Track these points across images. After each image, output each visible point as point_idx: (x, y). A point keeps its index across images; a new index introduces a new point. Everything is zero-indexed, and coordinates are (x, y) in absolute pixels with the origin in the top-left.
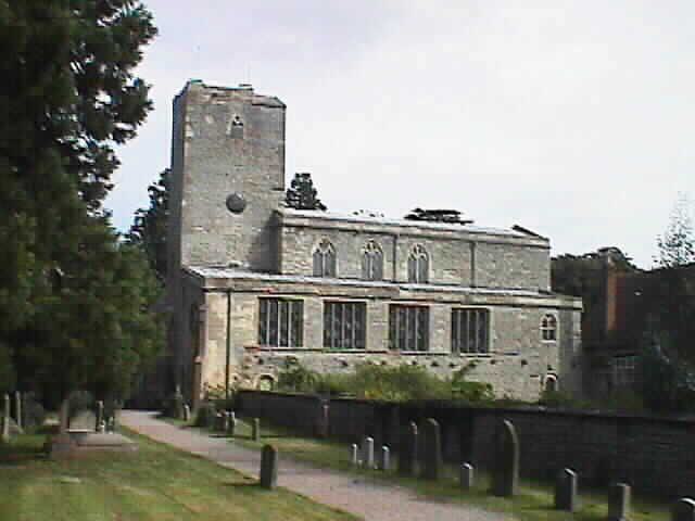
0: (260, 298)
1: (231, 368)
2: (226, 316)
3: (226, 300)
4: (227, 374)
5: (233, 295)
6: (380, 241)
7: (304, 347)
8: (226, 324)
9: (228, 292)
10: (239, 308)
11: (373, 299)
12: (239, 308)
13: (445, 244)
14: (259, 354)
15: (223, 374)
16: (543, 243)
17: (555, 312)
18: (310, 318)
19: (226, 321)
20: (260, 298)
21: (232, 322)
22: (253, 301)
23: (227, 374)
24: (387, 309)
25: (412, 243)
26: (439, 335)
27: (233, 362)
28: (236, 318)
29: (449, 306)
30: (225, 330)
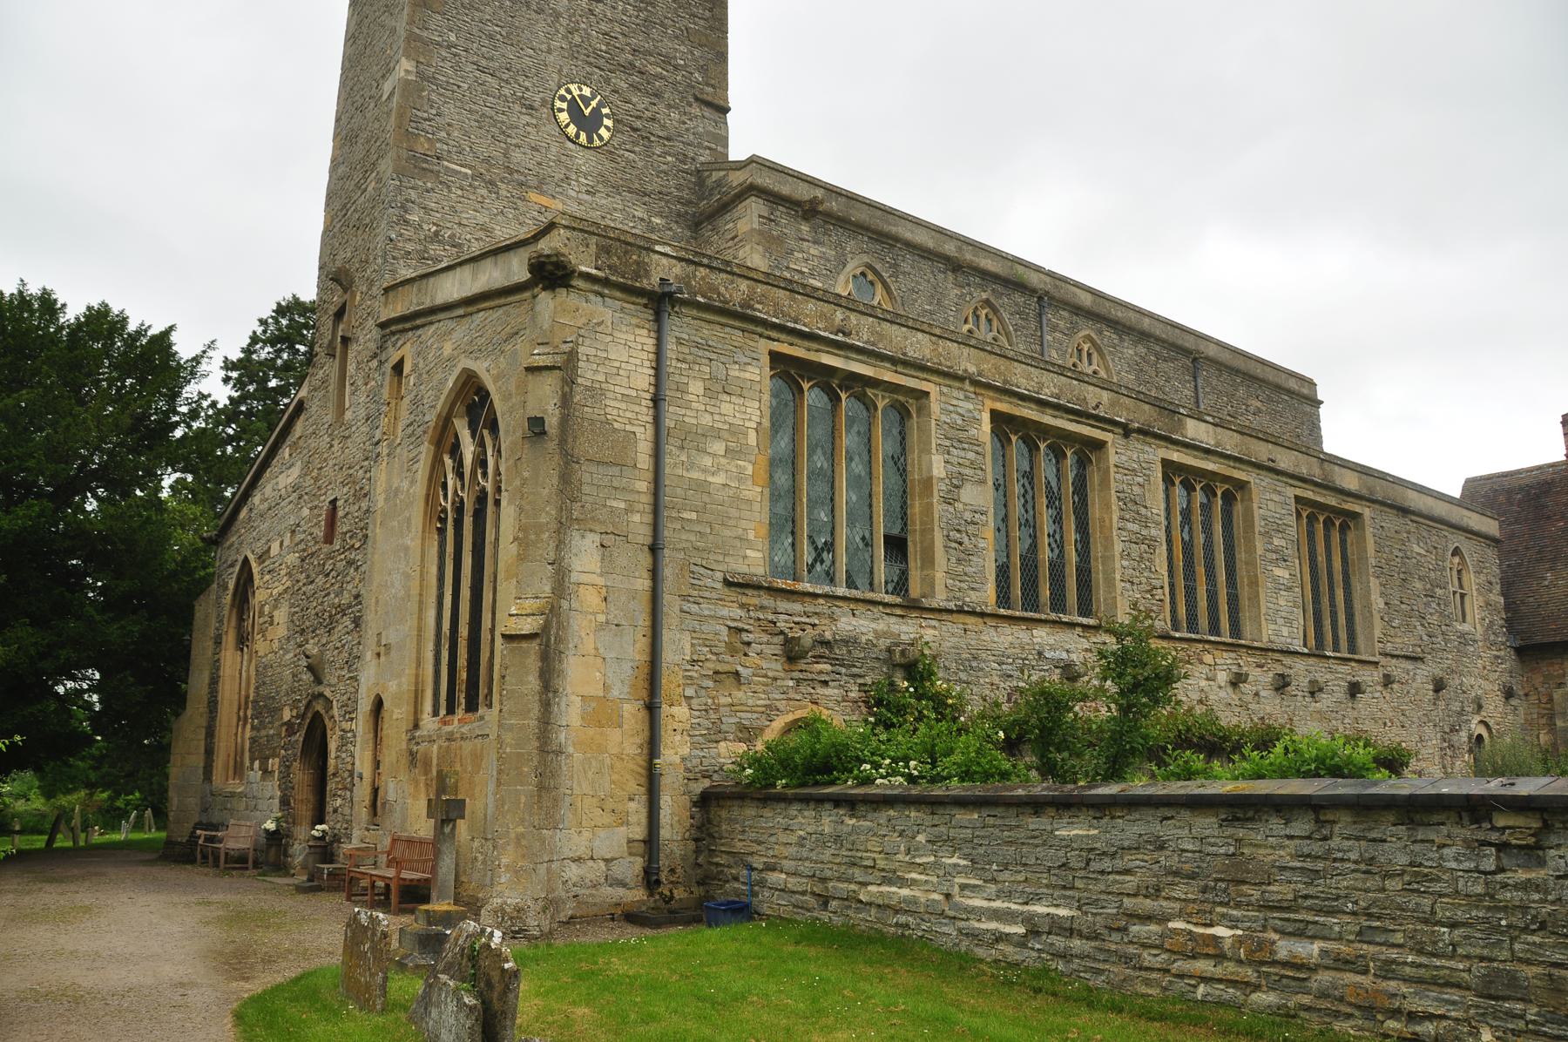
0: (776, 357)
1: (670, 681)
2: (646, 415)
3: (650, 343)
4: (652, 708)
5: (680, 326)
6: (1006, 303)
7: (940, 599)
8: (644, 461)
9: (660, 303)
10: (696, 387)
11: (1127, 432)
12: (696, 387)
13: (1142, 350)
14: (788, 614)
15: (632, 712)
16: (1305, 391)
17: (1466, 546)
18: (956, 483)
19: (644, 436)
20: (776, 357)
21: (670, 448)
22: (758, 373)
23: (652, 708)
24: (1158, 473)
25: (1074, 329)
26: (1279, 587)
27: (677, 647)
28: (695, 439)
29: (1290, 492)
30: (643, 486)
